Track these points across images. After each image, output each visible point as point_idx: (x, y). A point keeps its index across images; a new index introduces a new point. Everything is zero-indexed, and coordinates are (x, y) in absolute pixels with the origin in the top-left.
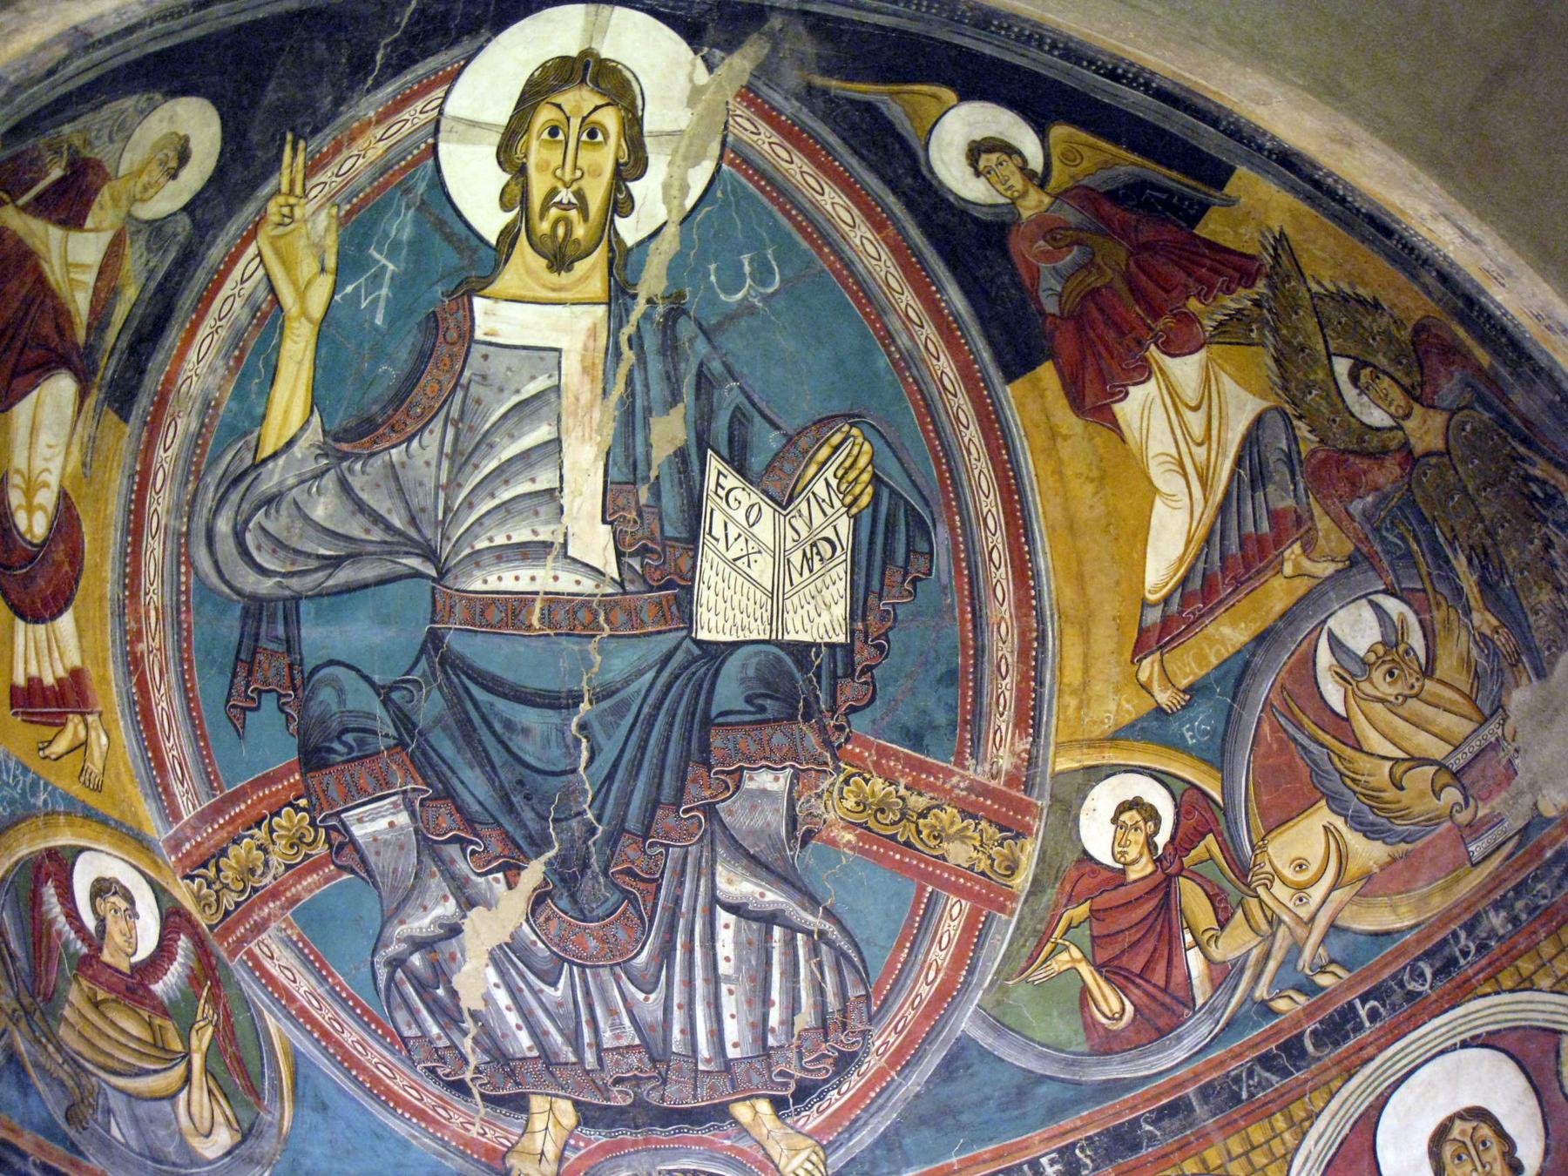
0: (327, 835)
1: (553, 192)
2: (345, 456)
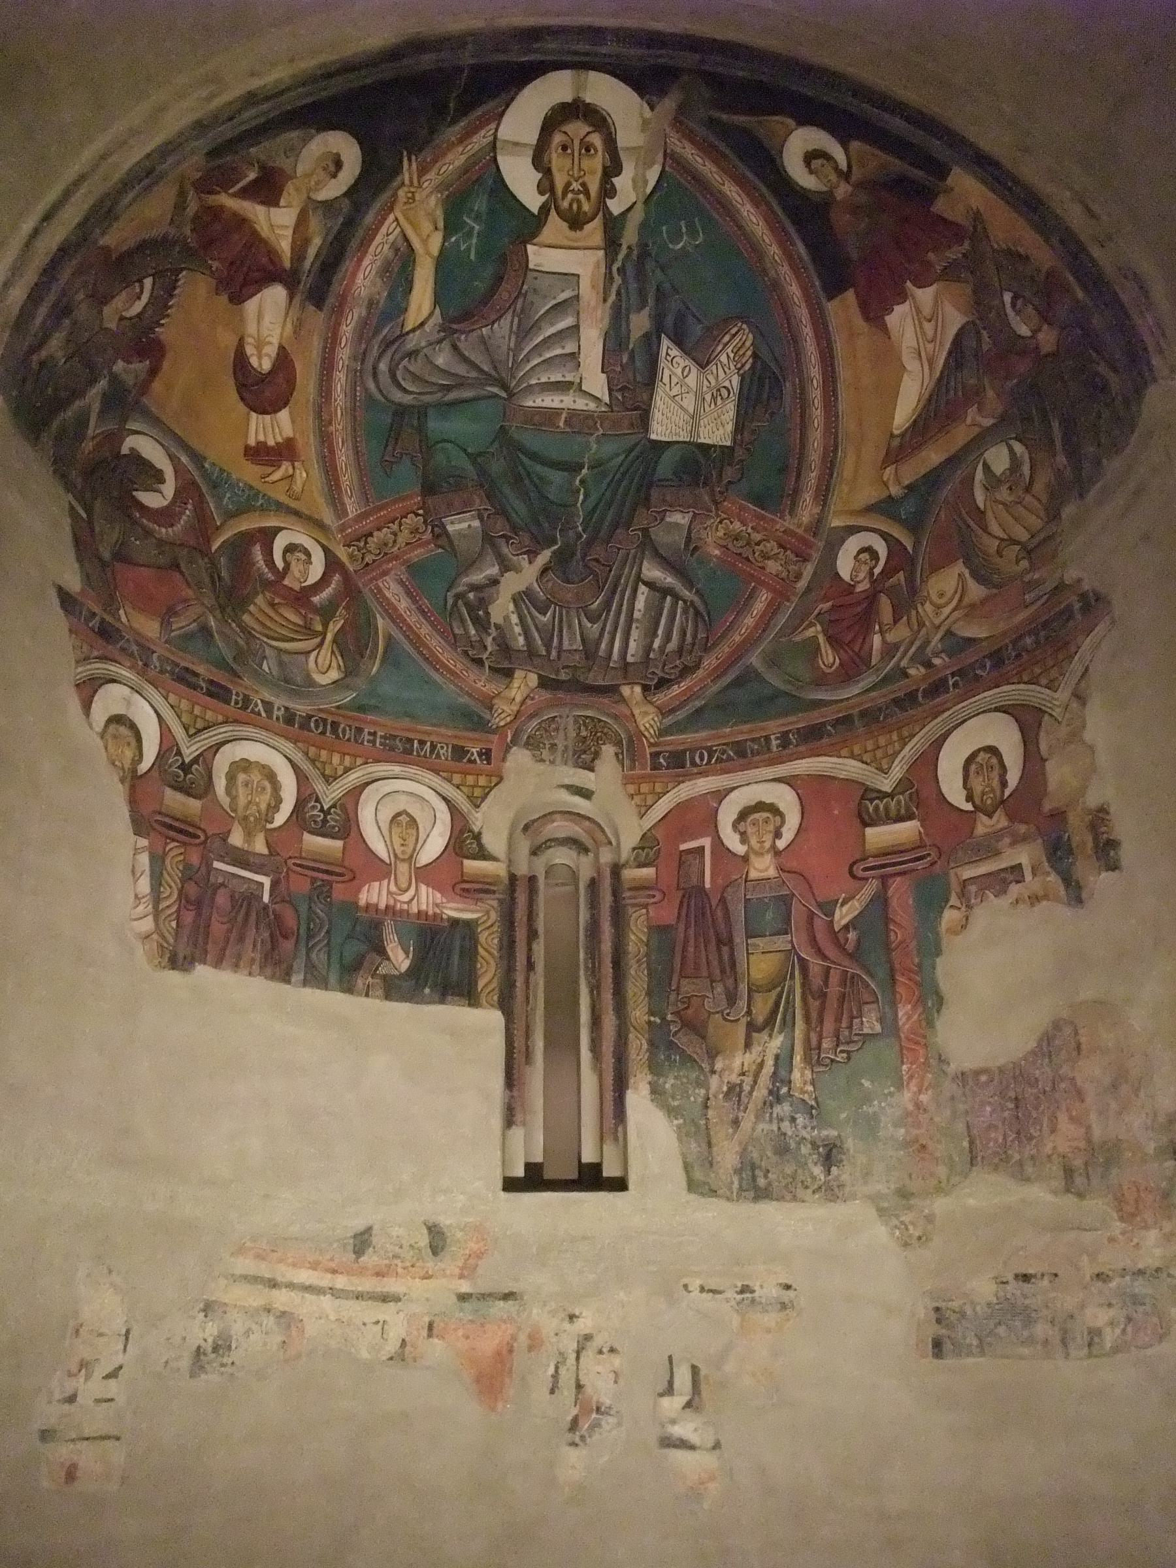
0: (433, 529)
1: (568, 184)
2: (455, 331)
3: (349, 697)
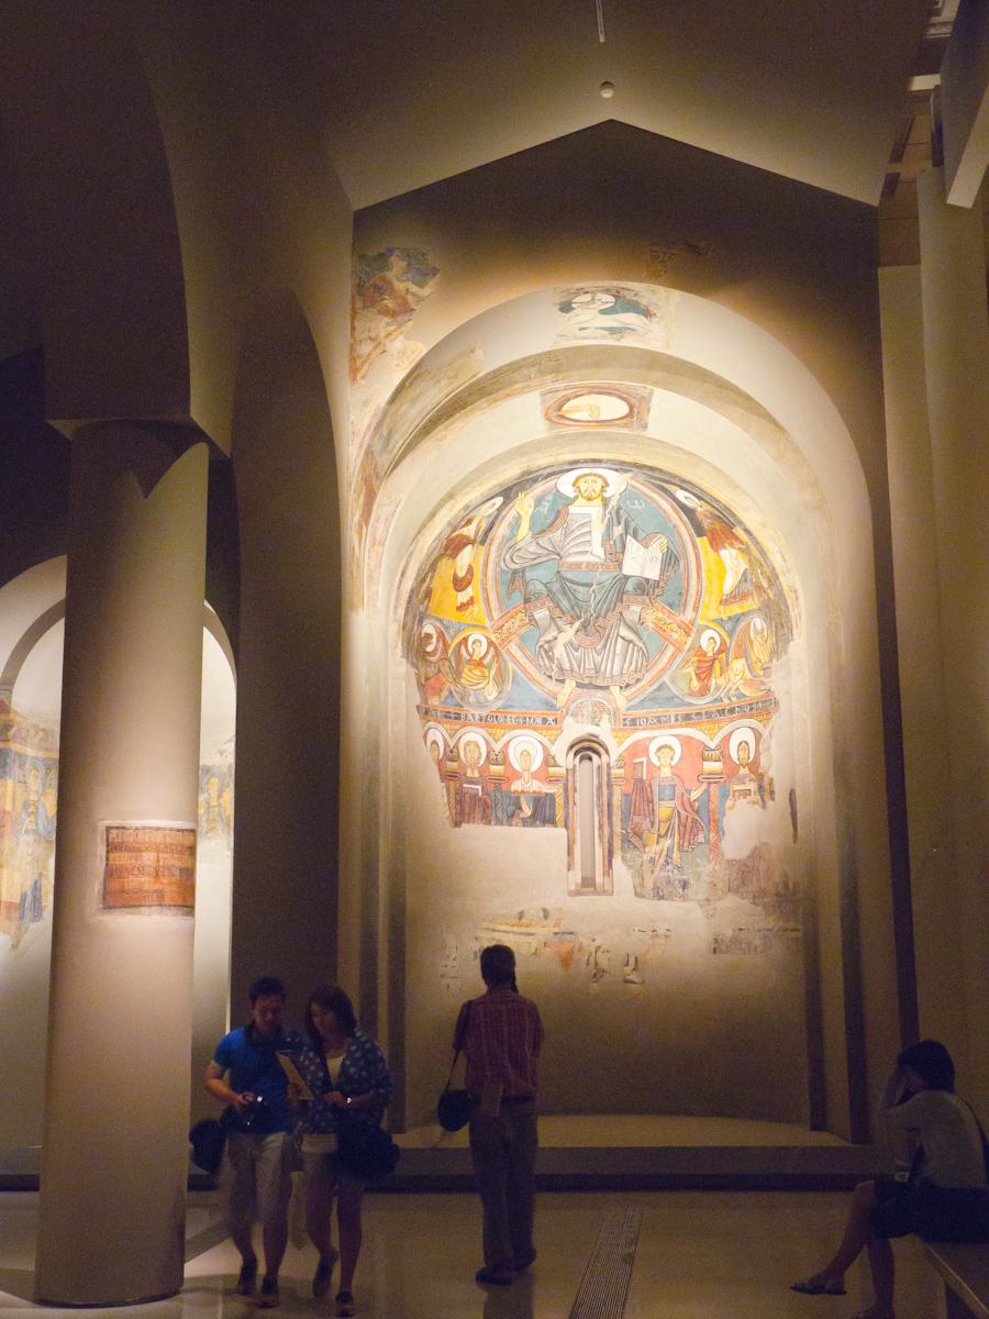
3: (500, 704)
